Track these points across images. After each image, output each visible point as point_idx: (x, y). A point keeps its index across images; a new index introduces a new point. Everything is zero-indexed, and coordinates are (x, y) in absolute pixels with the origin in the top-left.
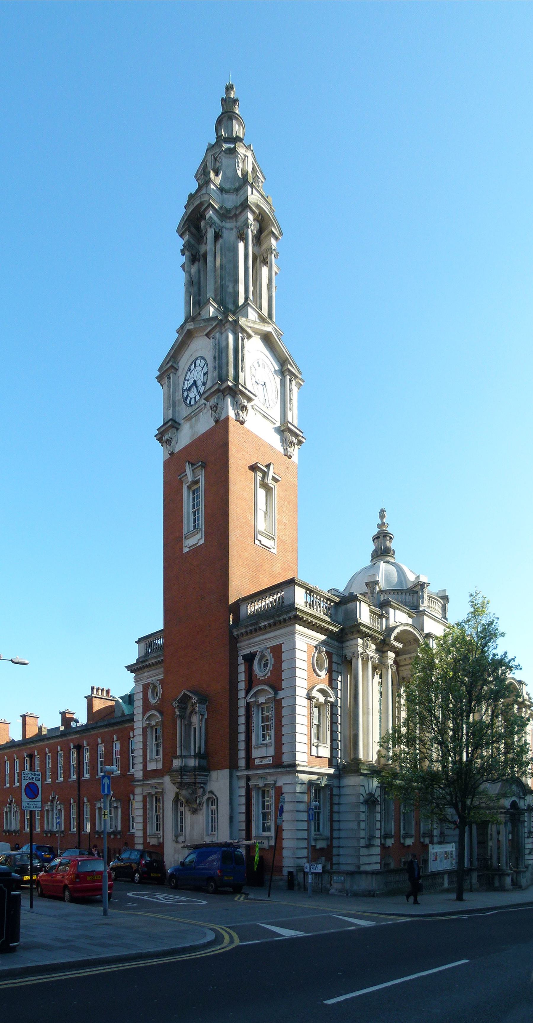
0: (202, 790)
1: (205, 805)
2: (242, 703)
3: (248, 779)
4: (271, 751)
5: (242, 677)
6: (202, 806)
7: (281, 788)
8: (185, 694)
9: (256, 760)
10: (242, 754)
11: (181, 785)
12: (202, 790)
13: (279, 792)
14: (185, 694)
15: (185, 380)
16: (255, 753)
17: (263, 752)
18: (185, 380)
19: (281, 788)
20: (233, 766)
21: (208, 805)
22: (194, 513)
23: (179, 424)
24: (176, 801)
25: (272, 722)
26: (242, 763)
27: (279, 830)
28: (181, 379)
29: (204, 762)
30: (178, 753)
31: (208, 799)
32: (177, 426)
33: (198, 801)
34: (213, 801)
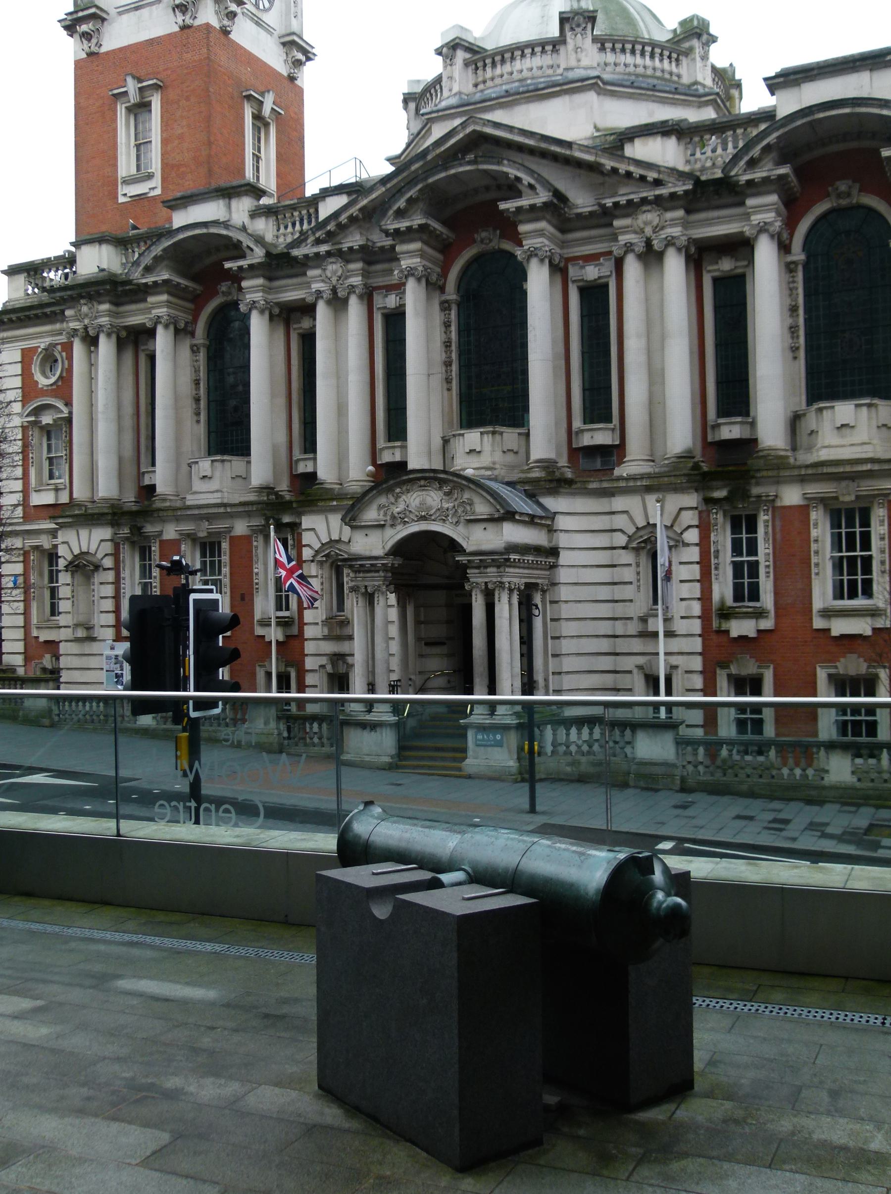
32: (104, 15)
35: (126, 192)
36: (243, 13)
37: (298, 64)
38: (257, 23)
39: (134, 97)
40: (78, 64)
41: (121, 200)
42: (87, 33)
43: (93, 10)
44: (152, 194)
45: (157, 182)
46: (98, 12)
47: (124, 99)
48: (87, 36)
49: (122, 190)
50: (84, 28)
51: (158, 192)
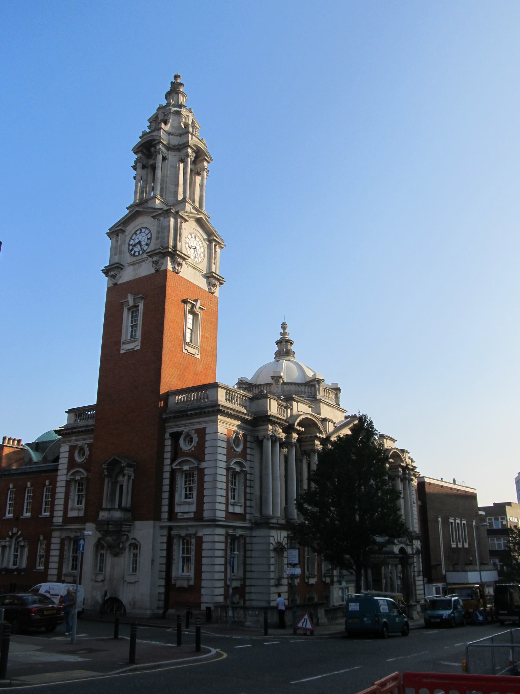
0: (125, 537)
1: (127, 550)
2: (167, 469)
4: (193, 508)
5: (168, 449)
6: (125, 550)
7: (201, 538)
8: (114, 459)
9: (179, 514)
10: (165, 509)
11: (106, 533)
12: (125, 537)
13: (200, 541)
14: (114, 459)
15: (131, 239)
16: (177, 509)
17: (185, 507)
18: (131, 239)
19: (201, 538)
21: (130, 550)
22: (132, 327)
23: (124, 266)
25: (195, 485)
26: (165, 516)
27: (198, 572)
30: (104, 506)
31: (131, 544)
33: (121, 546)
34: (135, 546)
35: (124, 348)
38: (194, 268)
39: (131, 303)
40: (108, 289)
41: (122, 352)
42: (113, 275)
48: (113, 277)
50: (112, 273)
51: (138, 348)
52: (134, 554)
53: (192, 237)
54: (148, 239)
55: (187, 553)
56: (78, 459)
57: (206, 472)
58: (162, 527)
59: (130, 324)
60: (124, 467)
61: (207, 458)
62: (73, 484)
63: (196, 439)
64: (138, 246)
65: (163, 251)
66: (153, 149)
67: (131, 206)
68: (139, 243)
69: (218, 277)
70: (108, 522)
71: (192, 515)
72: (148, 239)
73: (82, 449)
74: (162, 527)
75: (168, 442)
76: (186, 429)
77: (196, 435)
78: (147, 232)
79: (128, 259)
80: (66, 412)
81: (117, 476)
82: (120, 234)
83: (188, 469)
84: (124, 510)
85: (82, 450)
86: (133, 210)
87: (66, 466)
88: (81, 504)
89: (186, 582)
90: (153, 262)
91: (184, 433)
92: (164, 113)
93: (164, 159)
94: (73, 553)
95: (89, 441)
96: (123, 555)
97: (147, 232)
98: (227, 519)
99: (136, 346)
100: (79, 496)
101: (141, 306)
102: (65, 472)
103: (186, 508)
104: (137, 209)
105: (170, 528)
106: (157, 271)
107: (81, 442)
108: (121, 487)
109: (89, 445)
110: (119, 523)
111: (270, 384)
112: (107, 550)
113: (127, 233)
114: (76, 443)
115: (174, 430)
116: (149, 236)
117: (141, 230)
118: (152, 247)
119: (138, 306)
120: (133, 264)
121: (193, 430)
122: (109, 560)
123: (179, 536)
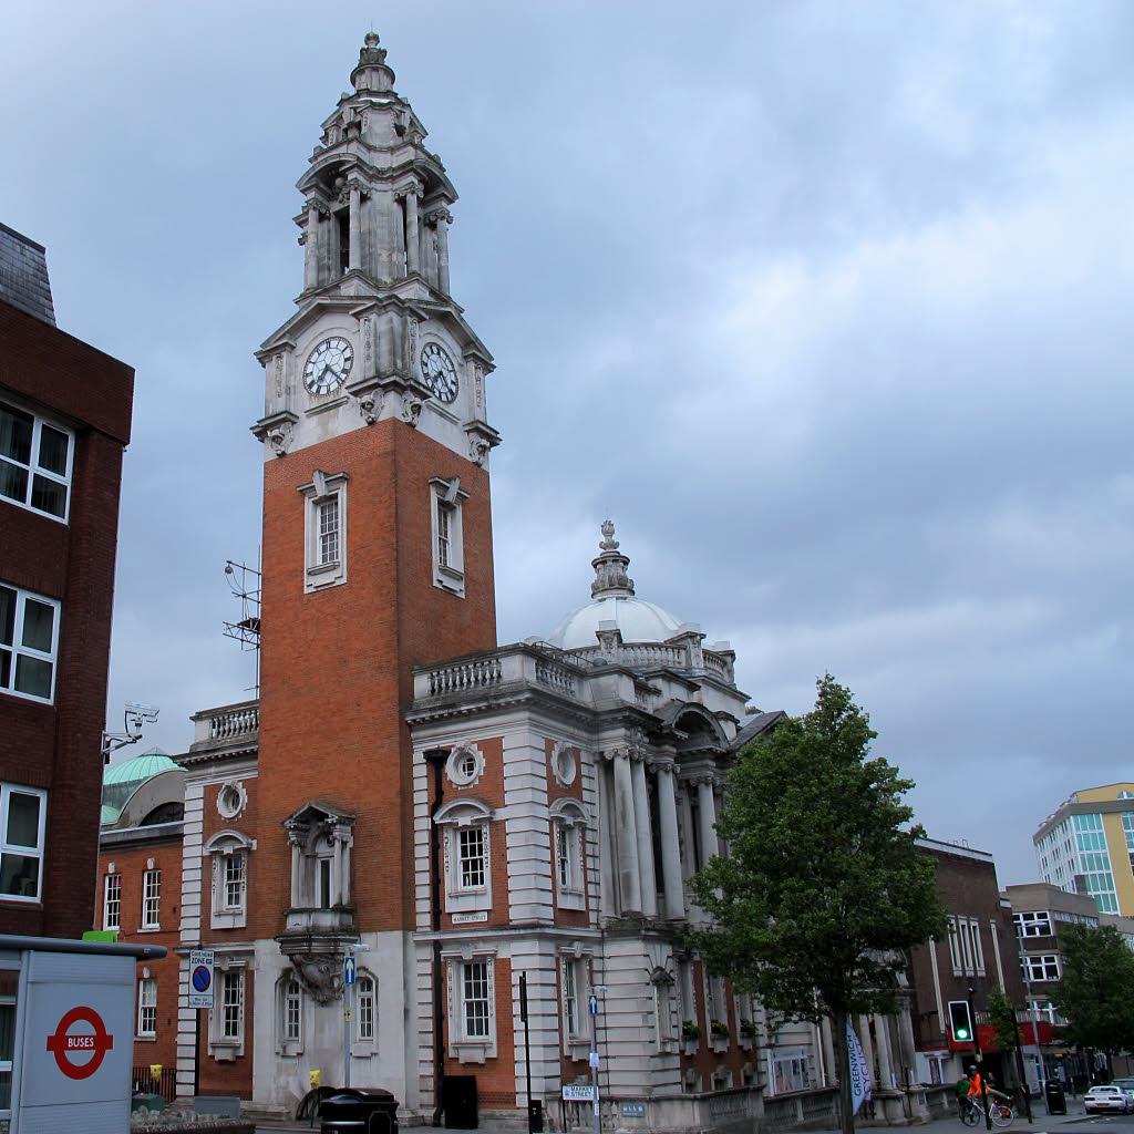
2: (422, 825)
3: (438, 945)
4: (487, 903)
8: (311, 808)
10: (424, 906)
14: (311, 808)
15: (308, 361)
16: (450, 906)
17: (467, 900)
18: (308, 361)
20: (408, 925)
22: (324, 539)
24: (287, 982)
26: (424, 920)
28: (303, 360)
29: (348, 919)
30: (294, 905)
32: (295, 420)
33: (336, 985)
35: (311, 584)
36: (428, 406)
37: (483, 450)
38: (441, 415)
42: (278, 437)
43: (284, 415)
44: (338, 583)
45: (343, 571)
46: (289, 416)
47: (312, 494)
49: (307, 580)
50: (276, 432)
51: (344, 580)
52: (291, 1002)
53: (432, 352)
54: (346, 360)
55: (478, 995)
56: (226, 812)
57: (509, 827)
58: (419, 944)
59: (319, 534)
60: (333, 824)
61: (508, 799)
62: (217, 862)
63: (480, 762)
64: (329, 376)
65: (382, 383)
66: (339, 181)
67: (304, 297)
68: (327, 369)
69: (488, 431)
70: (309, 935)
71: (484, 917)
72: (346, 360)
73: (232, 795)
74: (419, 944)
75: (421, 770)
76: (460, 743)
77: (481, 753)
78: (343, 345)
79: (302, 402)
80: (192, 718)
81: (314, 845)
82: (284, 354)
83: (469, 824)
84: (339, 909)
85: (232, 795)
86: (309, 305)
87: (200, 827)
88: (237, 903)
89: (482, 1051)
90: (363, 406)
91: (453, 750)
92: (355, 109)
93: (364, 199)
94: (227, 1000)
95: (245, 776)
96: (341, 1003)
97: (343, 345)
98: (557, 923)
99: (339, 576)
100: (230, 886)
101: (343, 494)
102: (199, 839)
103: (469, 904)
104: (319, 300)
105: (438, 945)
106: (372, 423)
107: (234, 777)
108: (326, 865)
109: (246, 783)
110: (332, 936)
111: (594, 649)
112: (304, 992)
113: (298, 351)
114: (218, 781)
115: (432, 746)
116: (348, 354)
117: (328, 342)
118: (356, 376)
119: (336, 496)
120: (312, 412)
121: (473, 743)
122: (309, 1011)
123: (459, 960)
